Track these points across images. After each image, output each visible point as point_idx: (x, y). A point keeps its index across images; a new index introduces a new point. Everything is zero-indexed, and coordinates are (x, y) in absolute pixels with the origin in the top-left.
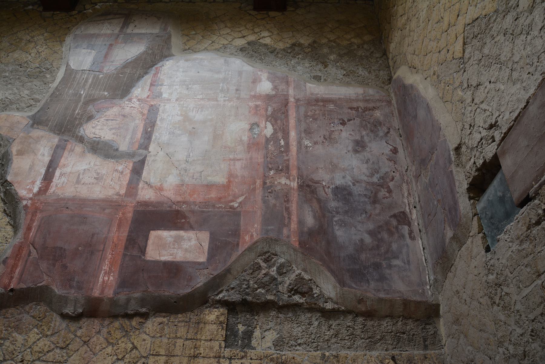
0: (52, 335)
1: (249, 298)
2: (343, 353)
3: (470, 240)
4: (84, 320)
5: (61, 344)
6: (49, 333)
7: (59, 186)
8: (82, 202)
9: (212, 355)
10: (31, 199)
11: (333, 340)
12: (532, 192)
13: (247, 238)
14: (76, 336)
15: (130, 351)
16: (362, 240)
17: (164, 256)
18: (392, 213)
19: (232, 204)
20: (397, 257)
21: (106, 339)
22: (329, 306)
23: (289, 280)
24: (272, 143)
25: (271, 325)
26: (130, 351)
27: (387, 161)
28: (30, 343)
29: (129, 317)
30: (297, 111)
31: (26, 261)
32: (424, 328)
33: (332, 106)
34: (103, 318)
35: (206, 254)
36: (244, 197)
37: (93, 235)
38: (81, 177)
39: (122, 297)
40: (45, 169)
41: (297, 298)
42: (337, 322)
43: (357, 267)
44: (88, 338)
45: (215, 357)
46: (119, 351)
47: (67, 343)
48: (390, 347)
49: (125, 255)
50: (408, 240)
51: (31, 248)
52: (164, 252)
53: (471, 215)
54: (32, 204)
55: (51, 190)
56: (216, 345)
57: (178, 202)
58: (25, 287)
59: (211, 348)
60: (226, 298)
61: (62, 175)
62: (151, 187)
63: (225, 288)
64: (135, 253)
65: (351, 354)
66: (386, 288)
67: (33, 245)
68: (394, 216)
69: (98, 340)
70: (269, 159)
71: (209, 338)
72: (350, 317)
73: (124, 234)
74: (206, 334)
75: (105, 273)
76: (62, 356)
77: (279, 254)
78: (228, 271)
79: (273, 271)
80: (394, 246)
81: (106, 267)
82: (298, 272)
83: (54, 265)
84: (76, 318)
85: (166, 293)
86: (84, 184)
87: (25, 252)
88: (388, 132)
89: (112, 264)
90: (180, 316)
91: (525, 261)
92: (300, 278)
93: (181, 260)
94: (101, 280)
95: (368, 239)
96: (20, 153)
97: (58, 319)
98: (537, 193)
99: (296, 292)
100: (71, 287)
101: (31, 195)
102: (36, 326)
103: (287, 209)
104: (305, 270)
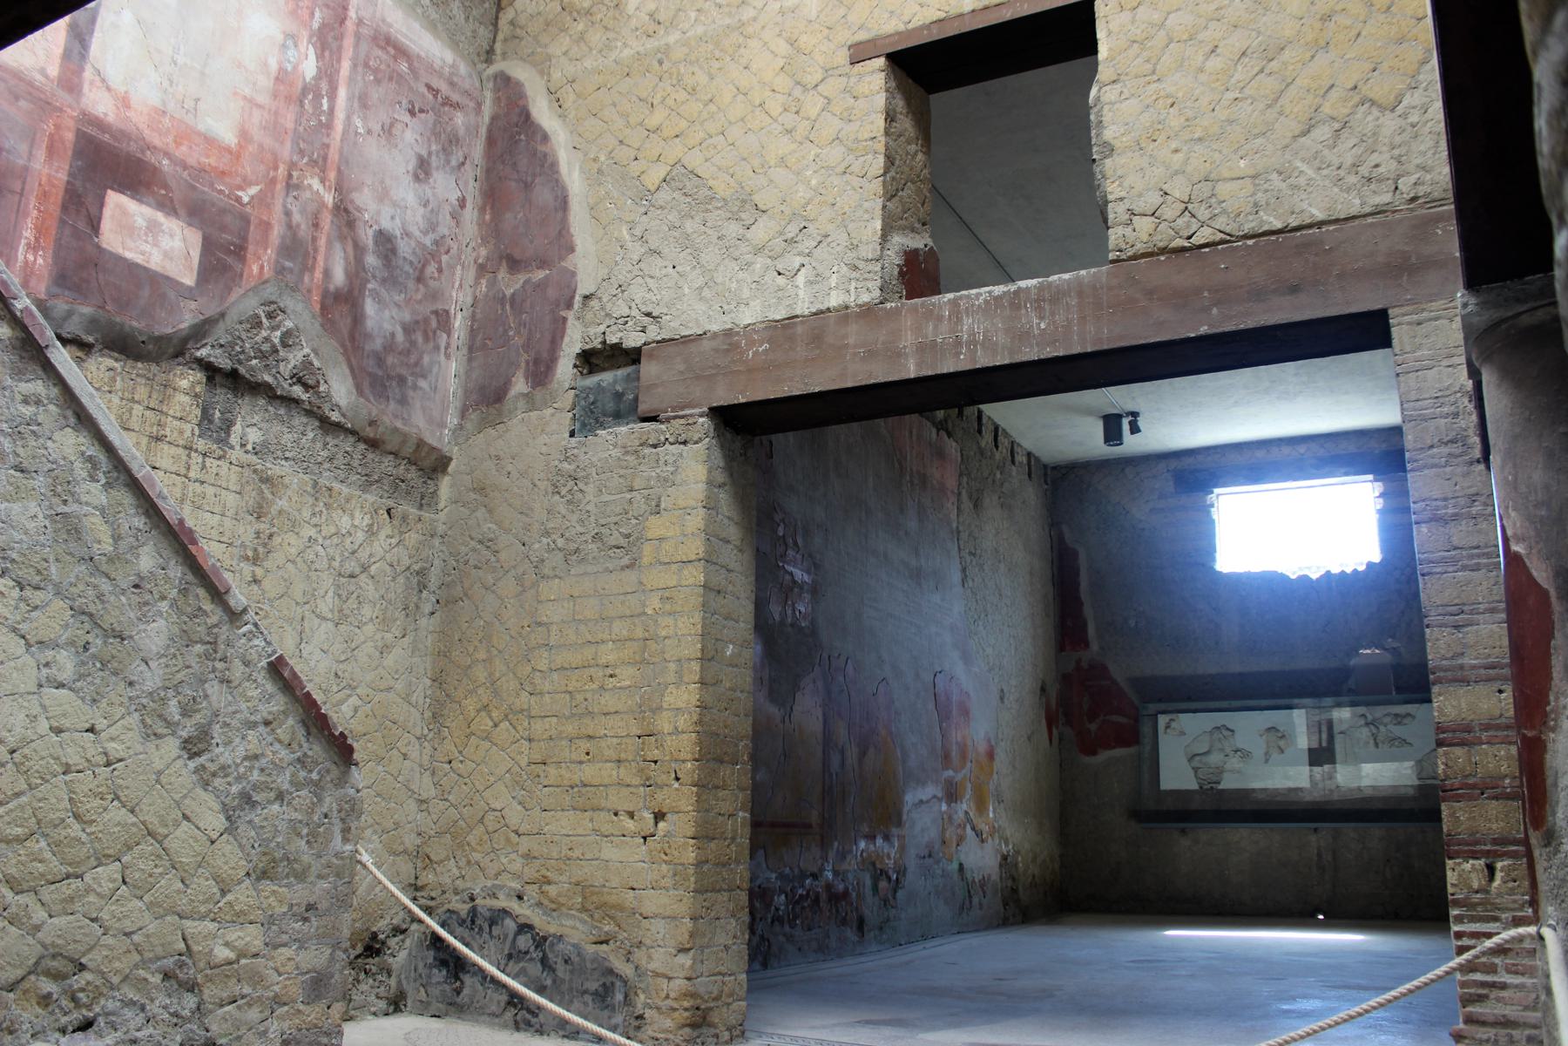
1: (242, 370)
2: (336, 486)
3: (549, 411)
9: (181, 442)
11: (327, 465)
12: (662, 416)
13: (255, 269)
16: (393, 335)
17: (130, 250)
18: (434, 308)
19: (240, 193)
20: (424, 376)
22: (335, 417)
23: (294, 358)
24: (310, 97)
25: (257, 418)
27: (448, 217)
30: (356, 46)
32: (425, 482)
33: (404, 67)
35: (195, 273)
36: (258, 188)
41: (297, 391)
42: (336, 442)
43: (380, 373)
45: (185, 448)
48: (386, 495)
49: (62, 222)
50: (442, 358)
53: (567, 386)
56: (188, 428)
57: (155, 148)
59: (181, 432)
60: (212, 359)
62: (109, 89)
63: (209, 340)
64: (82, 225)
65: (345, 490)
66: (405, 416)
68: (436, 313)
70: (301, 129)
71: (178, 415)
72: (351, 439)
74: (175, 410)
75: (28, 245)
77: (288, 311)
78: (223, 315)
79: (276, 337)
80: (426, 359)
81: (28, 234)
82: (307, 350)
85: (135, 324)
88: (463, 164)
89: (40, 231)
90: (140, 365)
91: (622, 472)
92: (307, 363)
93: (158, 269)
94: (21, 257)
95: (400, 337)
98: (668, 420)
99: (300, 381)
103: (314, 239)
104: (315, 351)
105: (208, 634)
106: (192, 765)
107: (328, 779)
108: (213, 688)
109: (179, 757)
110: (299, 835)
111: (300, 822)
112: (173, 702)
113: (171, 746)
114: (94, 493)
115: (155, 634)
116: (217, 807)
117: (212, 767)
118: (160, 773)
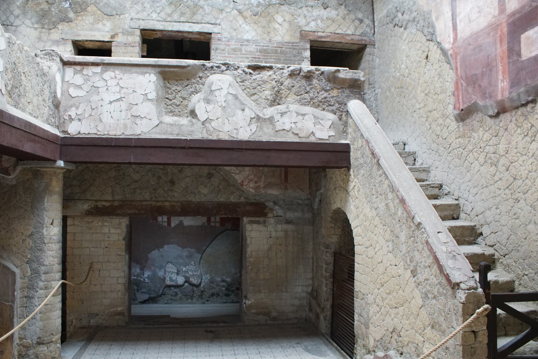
0: (489, 129)
4: (501, 115)
5: (495, 134)
6: (487, 129)
7: (461, 31)
8: (476, 36)
10: (452, 48)
14: (500, 127)
15: (531, 129)
21: (516, 124)
26: (531, 129)
28: (481, 137)
29: (525, 105)
31: (462, 90)
34: (511, 111)
37: (488, 56)
38: (470, 16)
39: (514, 95)
40: (451, 22)
44: (506, 127)
46: (524, 130)
47: (497, 132)
51: (462, 81)
52: (533, 49)
54: (454, 51)
55: (459, 37)
58: (466, 106)
61: (460, 21)
67: (461, 78)
69: (512, 126)
73: (505, 47)
76: (497, 141)
83: (475, 87)
84: (497, 115)
86: (473, 21)
87: (460, 85)
96: (437, 18)
97: (488, 119)
100: (486, 98)
101: (451, 46)
102: (481, 126)
105: (413, 234)
106: (414, 279)
107: (449, 294)
108: (416, 253)
109: (411, 277)
110: (441, 315)
111: (442, 310)
112: (408, 258)
113: (408, 273)
114: (390, 196)
115: (403, 237)
116: (420, 296)
117: (418, 281)
118: (407, 281)
